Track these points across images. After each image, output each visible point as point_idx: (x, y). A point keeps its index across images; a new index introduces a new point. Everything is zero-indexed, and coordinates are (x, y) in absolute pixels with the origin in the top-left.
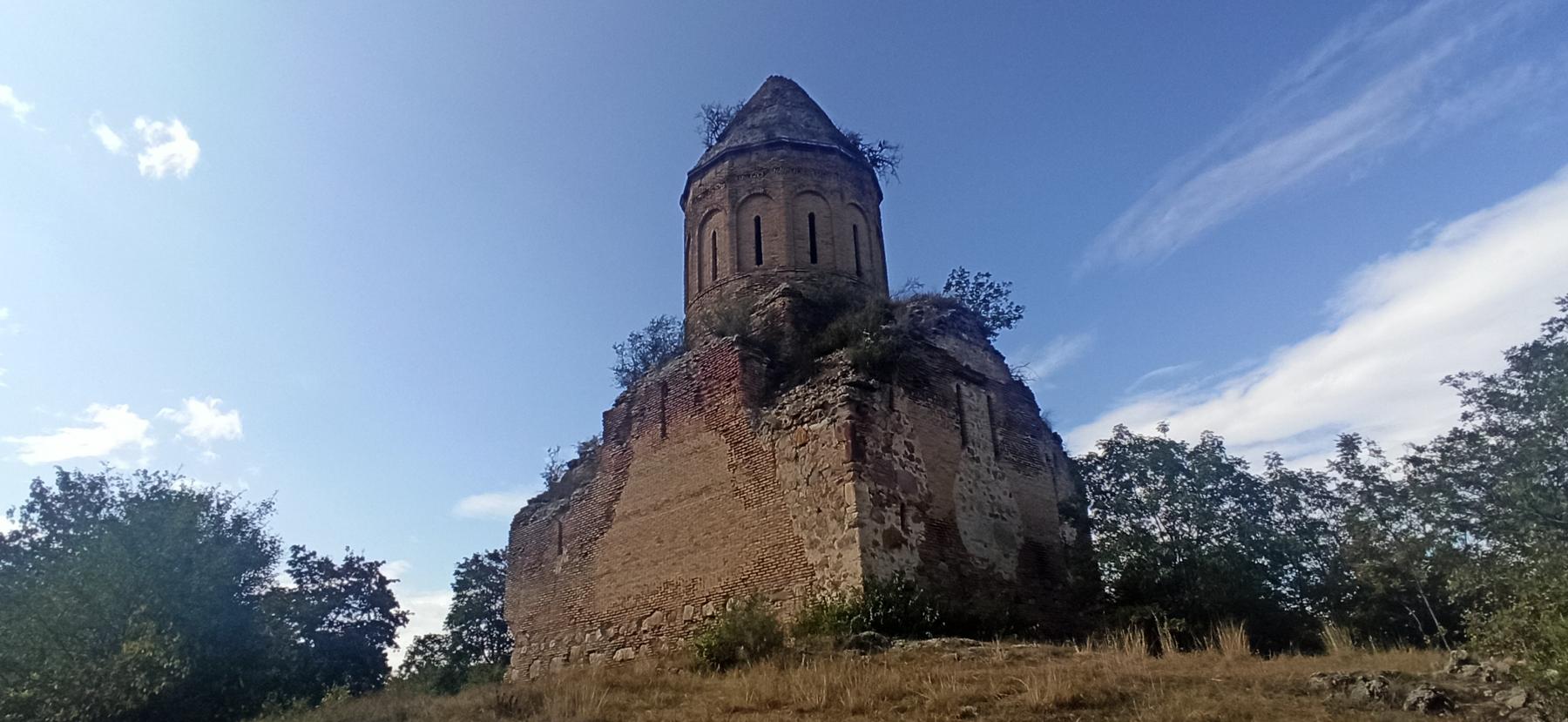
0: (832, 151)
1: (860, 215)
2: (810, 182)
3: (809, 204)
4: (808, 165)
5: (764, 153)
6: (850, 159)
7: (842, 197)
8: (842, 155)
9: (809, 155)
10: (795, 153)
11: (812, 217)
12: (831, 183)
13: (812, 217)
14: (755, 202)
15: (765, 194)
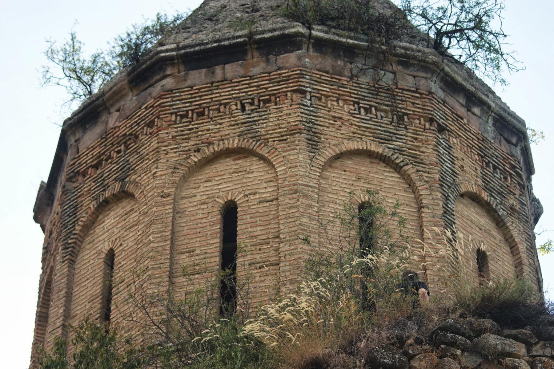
0: (287, 43)
1: (391, 178)
2: (226, 132)
3: (224, 182)
4: (225, 93)
5: (130, 101)
6: (350, 52)
7: (314, 144)
8: (320, 45)
9: (231, 70)
10: (198, 77)
11: (230, 214)
12: (289, 113)
13: (230, 214)
14: (111, 220)
15: (125, 195)
